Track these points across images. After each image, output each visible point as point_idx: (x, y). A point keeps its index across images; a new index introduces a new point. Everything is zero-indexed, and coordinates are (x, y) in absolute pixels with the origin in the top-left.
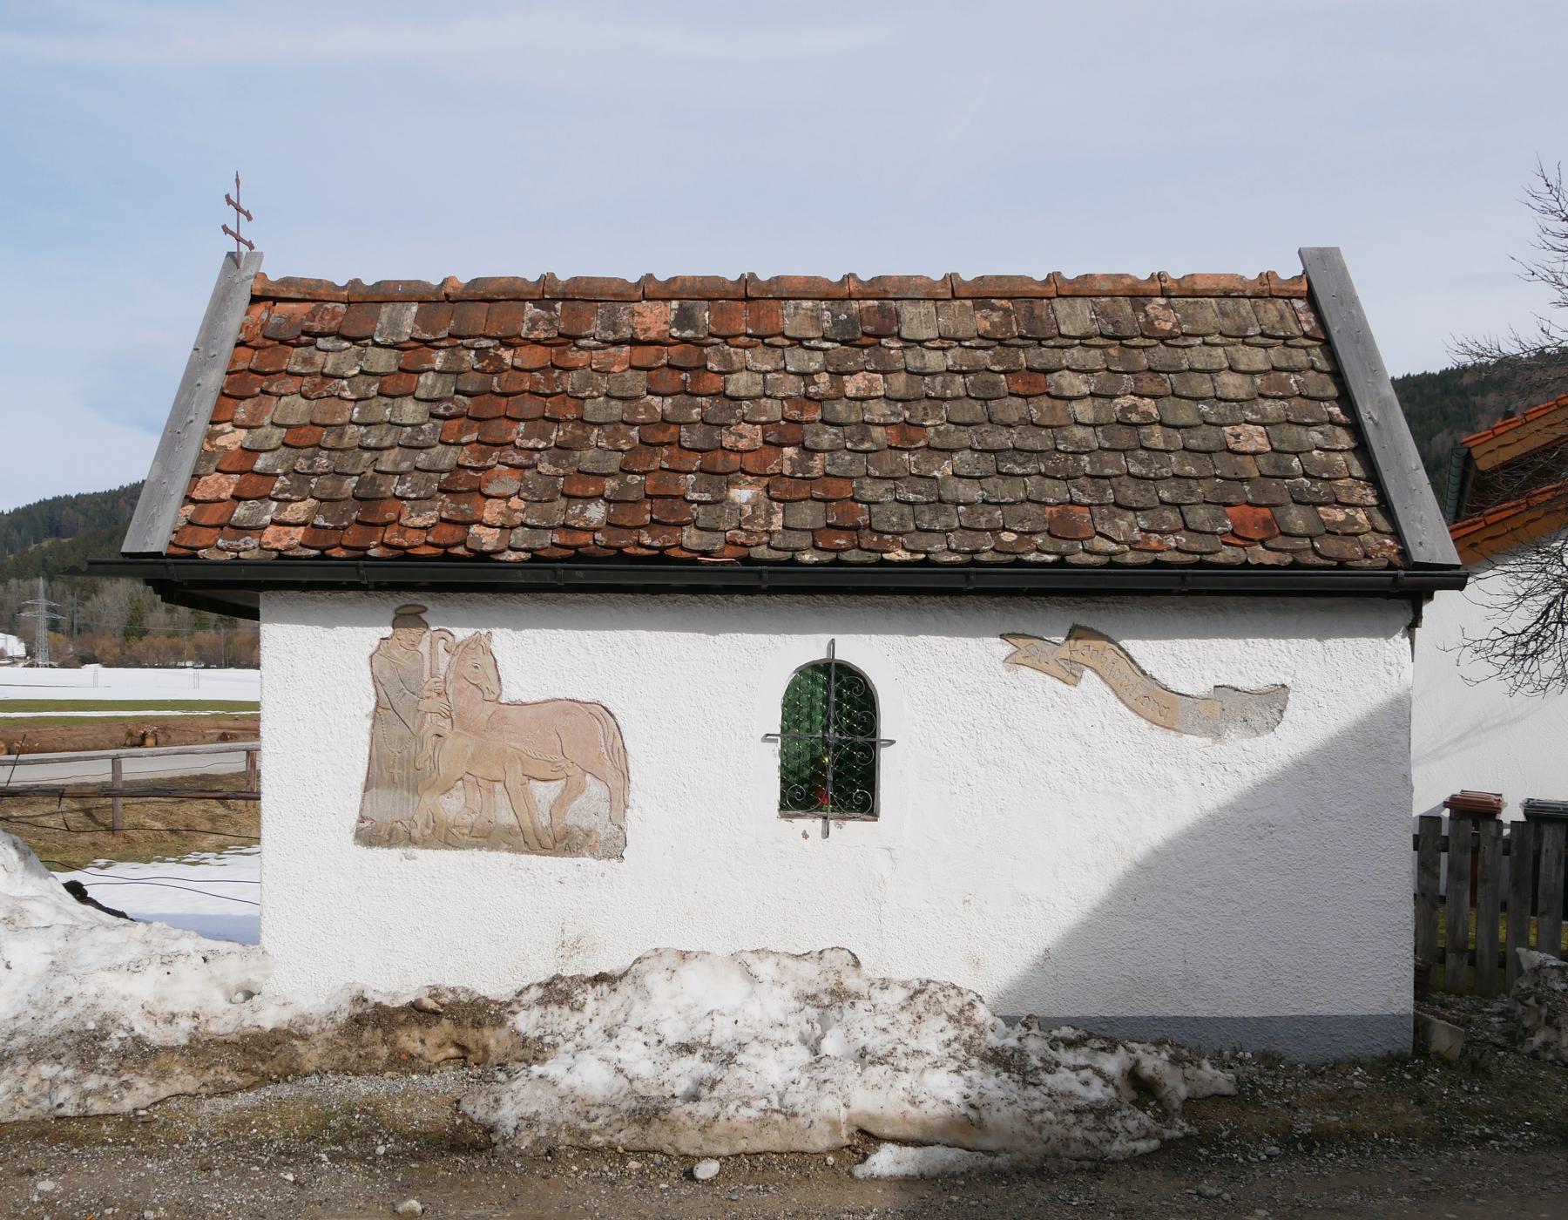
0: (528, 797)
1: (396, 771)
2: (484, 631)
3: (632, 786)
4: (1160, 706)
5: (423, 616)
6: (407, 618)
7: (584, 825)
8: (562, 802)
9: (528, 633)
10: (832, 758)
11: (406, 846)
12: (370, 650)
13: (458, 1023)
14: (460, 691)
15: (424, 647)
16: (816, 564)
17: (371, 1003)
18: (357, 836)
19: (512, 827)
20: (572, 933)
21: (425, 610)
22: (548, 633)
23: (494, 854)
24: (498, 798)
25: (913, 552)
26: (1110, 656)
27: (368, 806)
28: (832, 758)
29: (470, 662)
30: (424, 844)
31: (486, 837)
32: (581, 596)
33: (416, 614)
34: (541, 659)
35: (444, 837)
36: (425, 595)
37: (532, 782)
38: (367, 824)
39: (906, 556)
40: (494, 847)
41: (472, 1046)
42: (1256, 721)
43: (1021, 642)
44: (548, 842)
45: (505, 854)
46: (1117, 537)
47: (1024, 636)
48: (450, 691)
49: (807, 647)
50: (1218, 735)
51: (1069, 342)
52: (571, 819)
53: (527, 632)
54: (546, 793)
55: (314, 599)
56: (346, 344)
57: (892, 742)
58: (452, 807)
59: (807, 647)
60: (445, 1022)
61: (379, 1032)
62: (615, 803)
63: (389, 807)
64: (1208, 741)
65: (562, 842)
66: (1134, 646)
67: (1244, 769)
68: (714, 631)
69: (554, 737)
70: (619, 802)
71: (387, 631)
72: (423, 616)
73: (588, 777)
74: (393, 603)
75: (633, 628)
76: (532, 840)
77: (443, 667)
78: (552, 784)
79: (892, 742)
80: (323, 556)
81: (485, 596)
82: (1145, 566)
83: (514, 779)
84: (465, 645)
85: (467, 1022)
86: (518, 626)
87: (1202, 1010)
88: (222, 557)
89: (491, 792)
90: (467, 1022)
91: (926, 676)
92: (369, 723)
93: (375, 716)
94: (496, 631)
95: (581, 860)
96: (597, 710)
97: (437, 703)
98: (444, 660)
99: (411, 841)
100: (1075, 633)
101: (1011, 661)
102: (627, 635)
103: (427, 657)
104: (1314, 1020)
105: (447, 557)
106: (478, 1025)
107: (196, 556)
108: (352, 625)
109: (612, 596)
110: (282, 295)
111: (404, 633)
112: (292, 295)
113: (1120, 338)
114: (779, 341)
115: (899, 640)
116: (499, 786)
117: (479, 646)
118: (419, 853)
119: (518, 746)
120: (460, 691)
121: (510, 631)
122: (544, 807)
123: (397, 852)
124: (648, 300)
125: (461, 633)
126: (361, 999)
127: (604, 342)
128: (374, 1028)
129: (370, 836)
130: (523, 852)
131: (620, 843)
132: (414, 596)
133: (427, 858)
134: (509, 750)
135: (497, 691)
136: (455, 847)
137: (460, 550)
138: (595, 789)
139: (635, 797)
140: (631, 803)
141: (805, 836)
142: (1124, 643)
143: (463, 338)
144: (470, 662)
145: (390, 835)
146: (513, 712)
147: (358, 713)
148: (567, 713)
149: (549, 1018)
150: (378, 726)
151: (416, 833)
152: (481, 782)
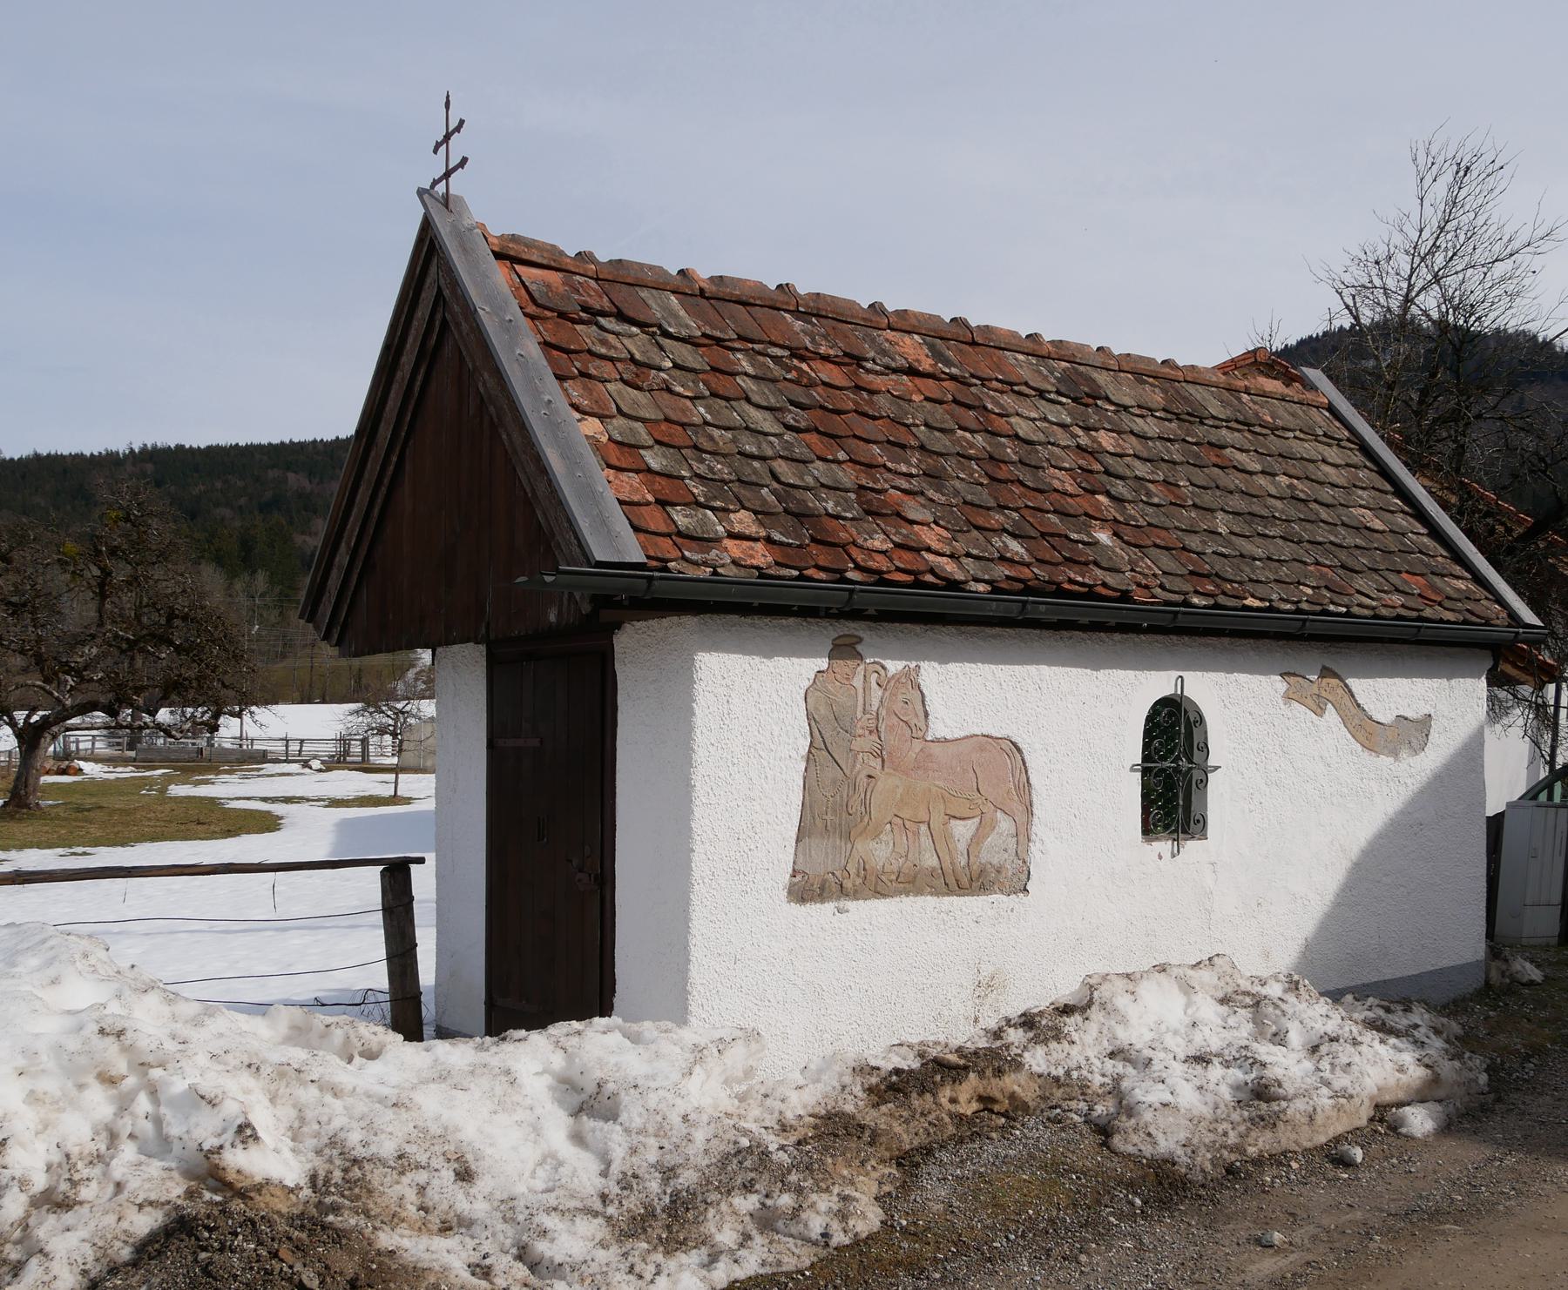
0: (948, 837)
1: (829, 817)
2: (913, 665)
3: (1035, 820)
4: (1369, 733)
5: (859, 648)
6: (844, 650)
7: (995, 861)
8: (977, 839)
9: (954, 667)
10: (1172, 786)
11: (838, 899)
12: (807, 684)
13: (981, 1074)
14: (891, 728)
15: (858, 682)
16: (1205, 607)
17: (847, 1079)
18: (790, 892)
19: (934, 869)
20: (987, 970)
21: (860, 640)
22: (968, 667)
23: (920, 899)
24: (923, 839)
25: (1261, 600)
26: (1340, 691)
27: (801, 859)
28: (1172, 786)
29: (900, 697)
30: (856, 895)
31: (910, 882)
32: (998, 630)
33: (852, 646)
34: (964, 693)
35: (875, 885)
36: (863, 624)
37: (953, 822)
38: (799, 878)
39: (1257, 603)
40: (919, 892)
41: (998, 1095)
42: (1415, 742)
43: (1292, 679)
44: (965, 881)
45: (929, 898)
46: (1369, 595)
47: (1294, 675)
48: (882, 729)
49: (1157, 684)
50: (1395, 754)
51: (1217, 423)
52: (985, 856)
53: (952, 666)
54: (962, 831)
55: (752, 625)
56: (635, 329)
57: (1217, 768)
58: (880, 852)
59: (1157, 684)
60: (972, 1075)
61: (928, 1096)
62: (1021, 837)
63: (824, 858)
64: (1391, 759)
65: (973, 880)
66: (1361, 687)
67: (1409, 781)
68: (1096, 667)
69: (972, 774)
70: (1023, 835)
71: (823, 663)
72: (859, 648)
73: (999, 814)
74: (833, 631)
75: (1038, 663)
76: (951, 881)
77: (876, 703)
78: (969, 822)
79: (1217, 768)
80: (801, 577)
81: (918, 628)
82: (1314, 613)
83: (937, 819)
84: (896, 678)
85: (989, 1072)
86: (944, 660)
87: (1445, 963)
88: (692, 572)
89: (917, 834)
90: (989, 1072)
91: (1241, 706)
92: (803, 765)
93: (810, 757)
94: (924, 665)
95: (993, 897)
96: (1007, 745)
97: (869, 742)
98: (877, 693)
99: (843, 892)
100: (1326, 672)
101: (1288, 697)
102: (1032, 669)
103: (860, 691)
104: (1441, 972)
105: (919, 584)
106: (999, 1072)
107: (666, 569)
108: (790, 656)
109: (1023, 631)
110: (525, 257)
111: (839, 664)
112: (534, 258)
113: (1248, 425)
114: (1024, 389)
115: (1219, 677)
116: (924, 828)
117: (910, 680)
118: (851, 905)
119: (941, 784)
120: (891, 728)
121: (936, 665)
122: (962, 846)
123: (830, 906)
124: (893, 329)
125: (894, 666)
126: (863, 1069)
127: (887, 367)
128: (921, 1094)
129: (805, 890)
130: (944, 894)
131: (1024, 877)
132: (852, 624)
133: (859, 910)
134: (934, 789)
135: (921, 724)
136: (884, 896)
137: (929, 578)
138: (1005, 825)
139: (1038, 829)
140: (1033, 837)
141: (1160, 857)
142: (1350, 681)
143: (752, 341)
144: (900, 697)
145: (822, 888)
146: (936, 749)
147: (794, 754)
148: (982, 749)
149: (1055, 1055)
150: (812, 767)
151: (848, 884)
152: (908, 824)
